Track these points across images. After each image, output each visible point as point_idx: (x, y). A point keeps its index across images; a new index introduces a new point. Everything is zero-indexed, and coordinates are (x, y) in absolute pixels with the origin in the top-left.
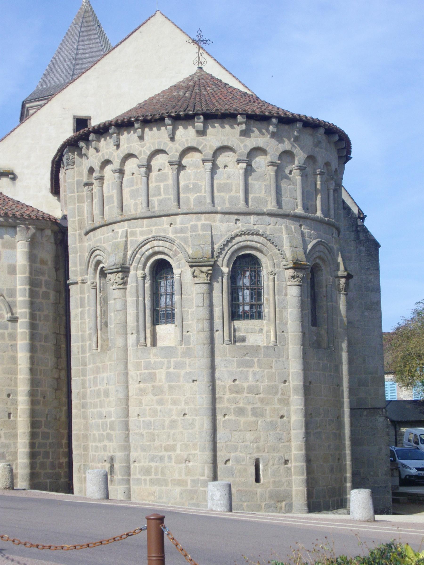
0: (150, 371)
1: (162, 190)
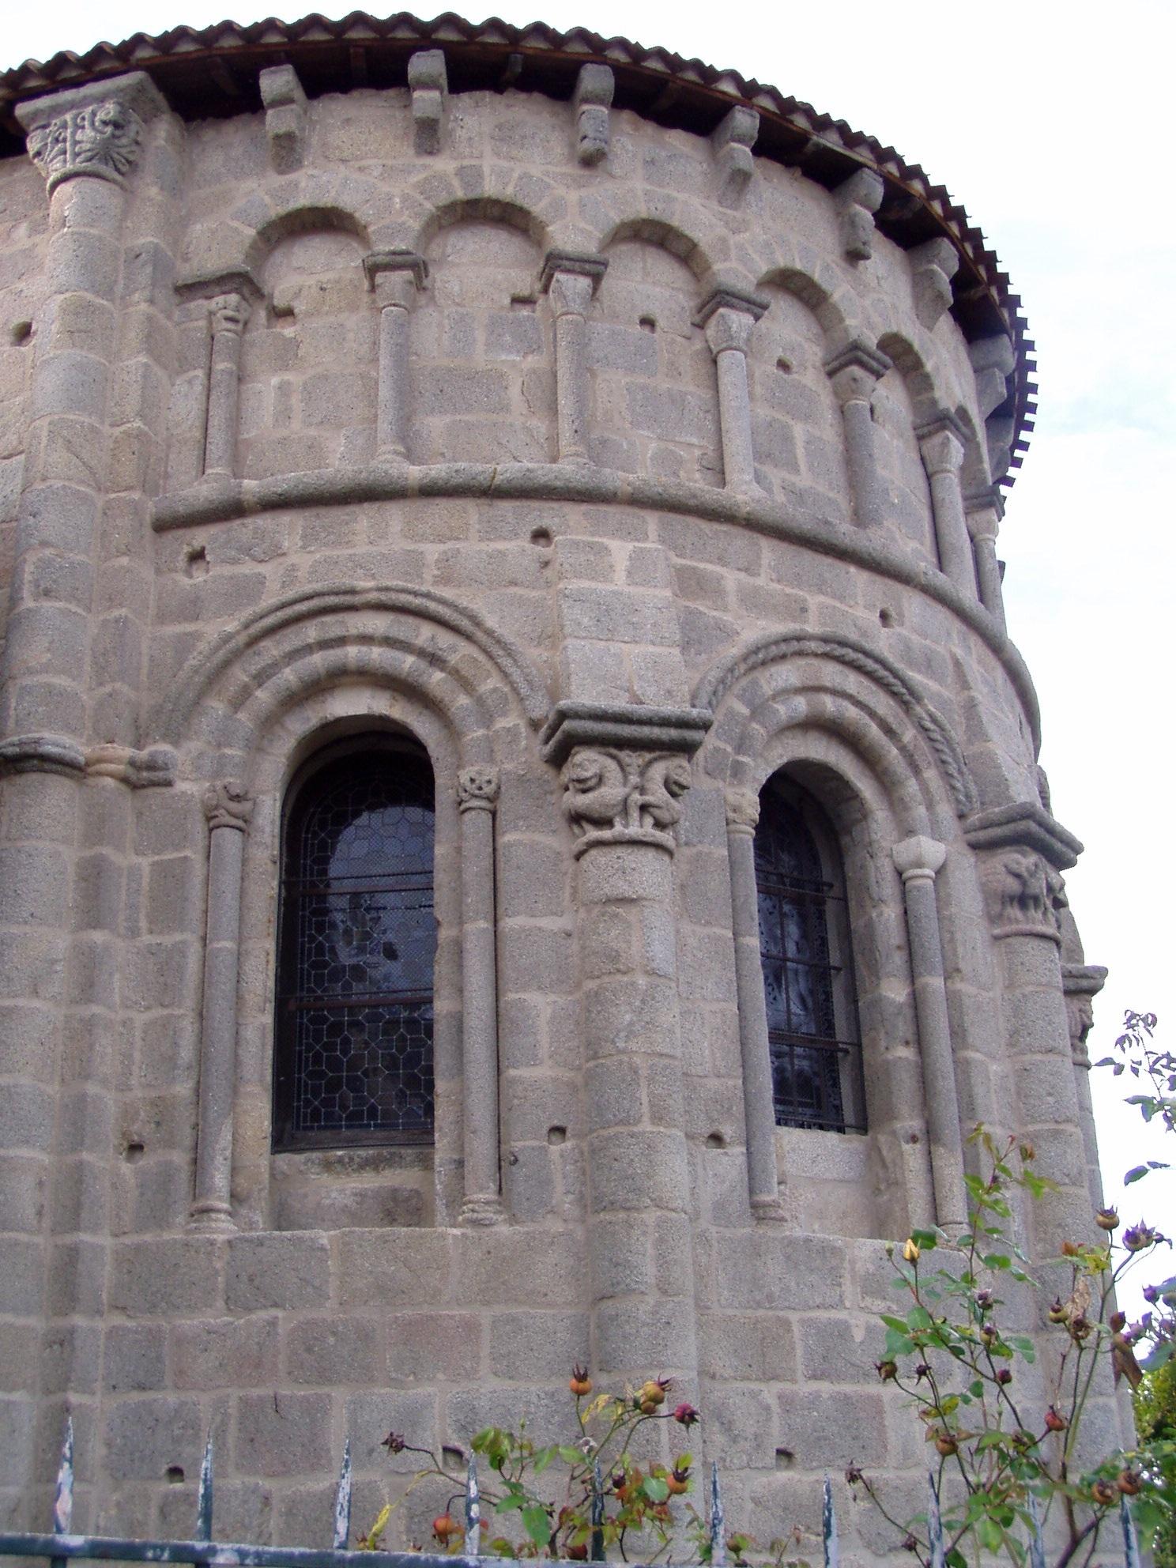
0: (847, 1388)
1: (800, 452)
